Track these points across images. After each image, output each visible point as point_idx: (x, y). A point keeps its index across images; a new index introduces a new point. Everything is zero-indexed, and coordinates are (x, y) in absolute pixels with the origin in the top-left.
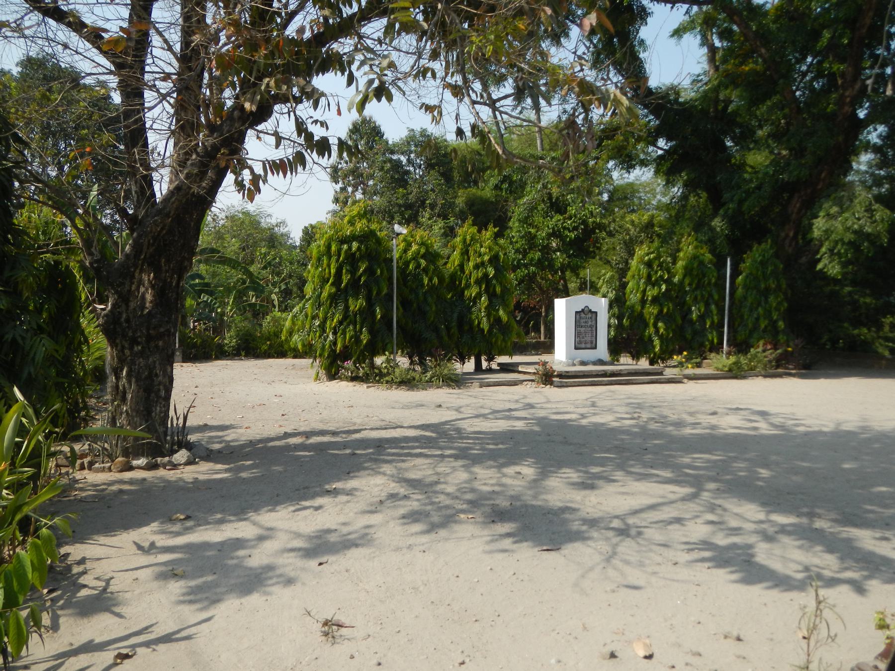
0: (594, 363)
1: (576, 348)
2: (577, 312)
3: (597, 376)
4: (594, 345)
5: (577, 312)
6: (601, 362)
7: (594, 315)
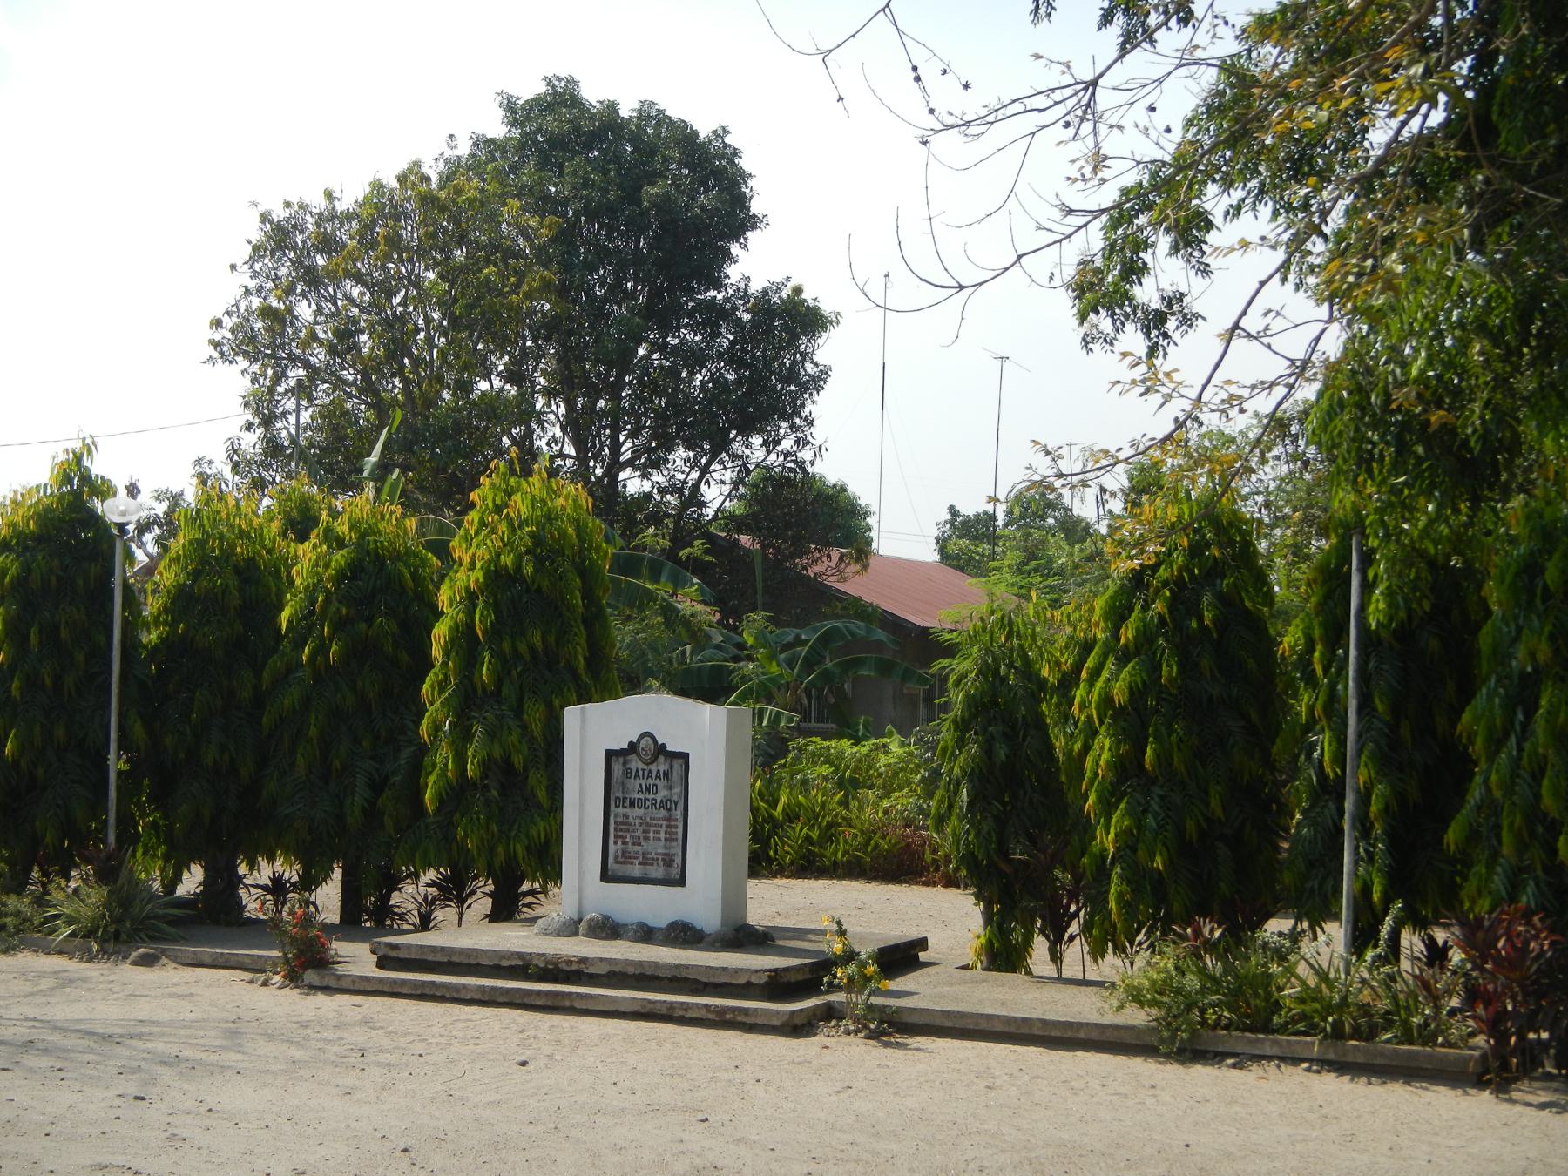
0: (646, 934)
1: (606, 876)
2: (610, 755)
3: (497, 971)
4: (675, 872)
5: (610, 755)
6: (683, 934)
7: (677, 764)
